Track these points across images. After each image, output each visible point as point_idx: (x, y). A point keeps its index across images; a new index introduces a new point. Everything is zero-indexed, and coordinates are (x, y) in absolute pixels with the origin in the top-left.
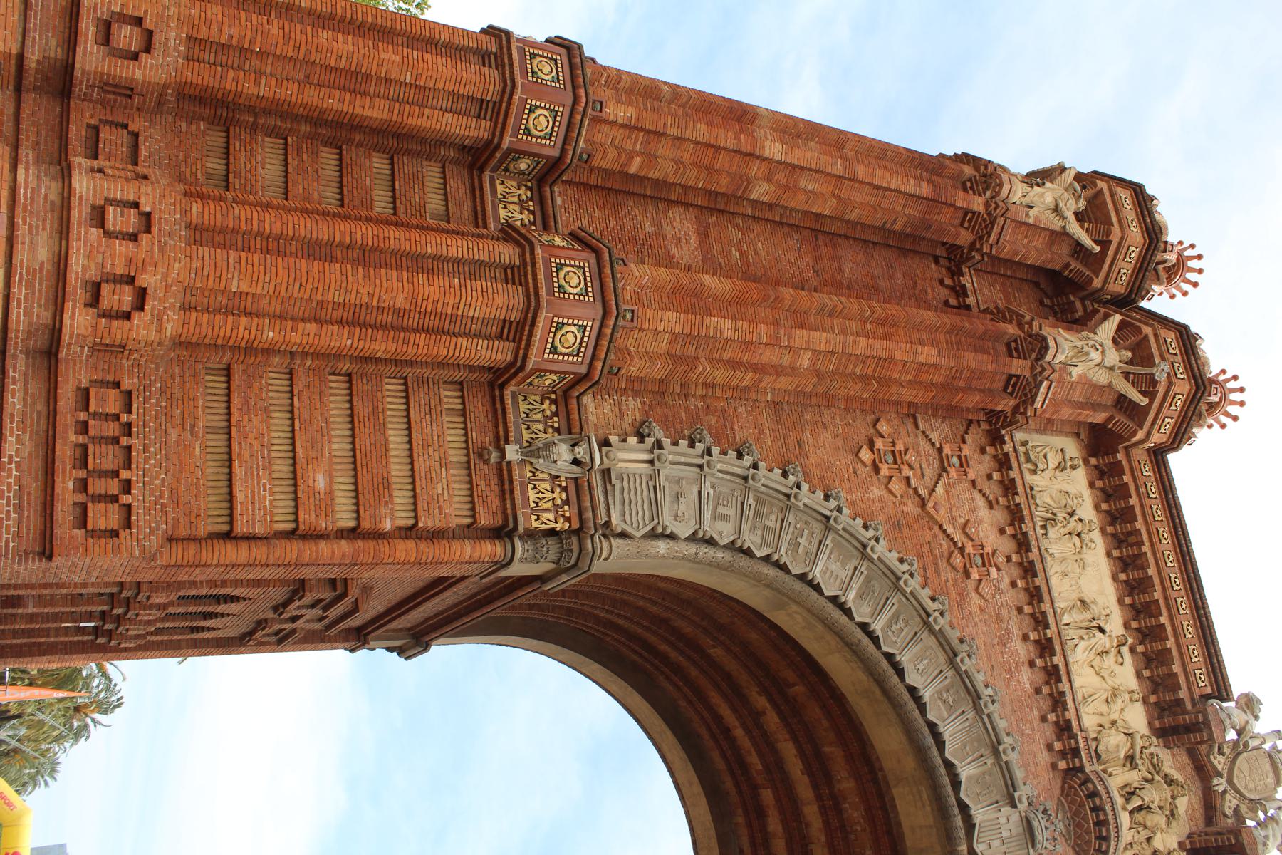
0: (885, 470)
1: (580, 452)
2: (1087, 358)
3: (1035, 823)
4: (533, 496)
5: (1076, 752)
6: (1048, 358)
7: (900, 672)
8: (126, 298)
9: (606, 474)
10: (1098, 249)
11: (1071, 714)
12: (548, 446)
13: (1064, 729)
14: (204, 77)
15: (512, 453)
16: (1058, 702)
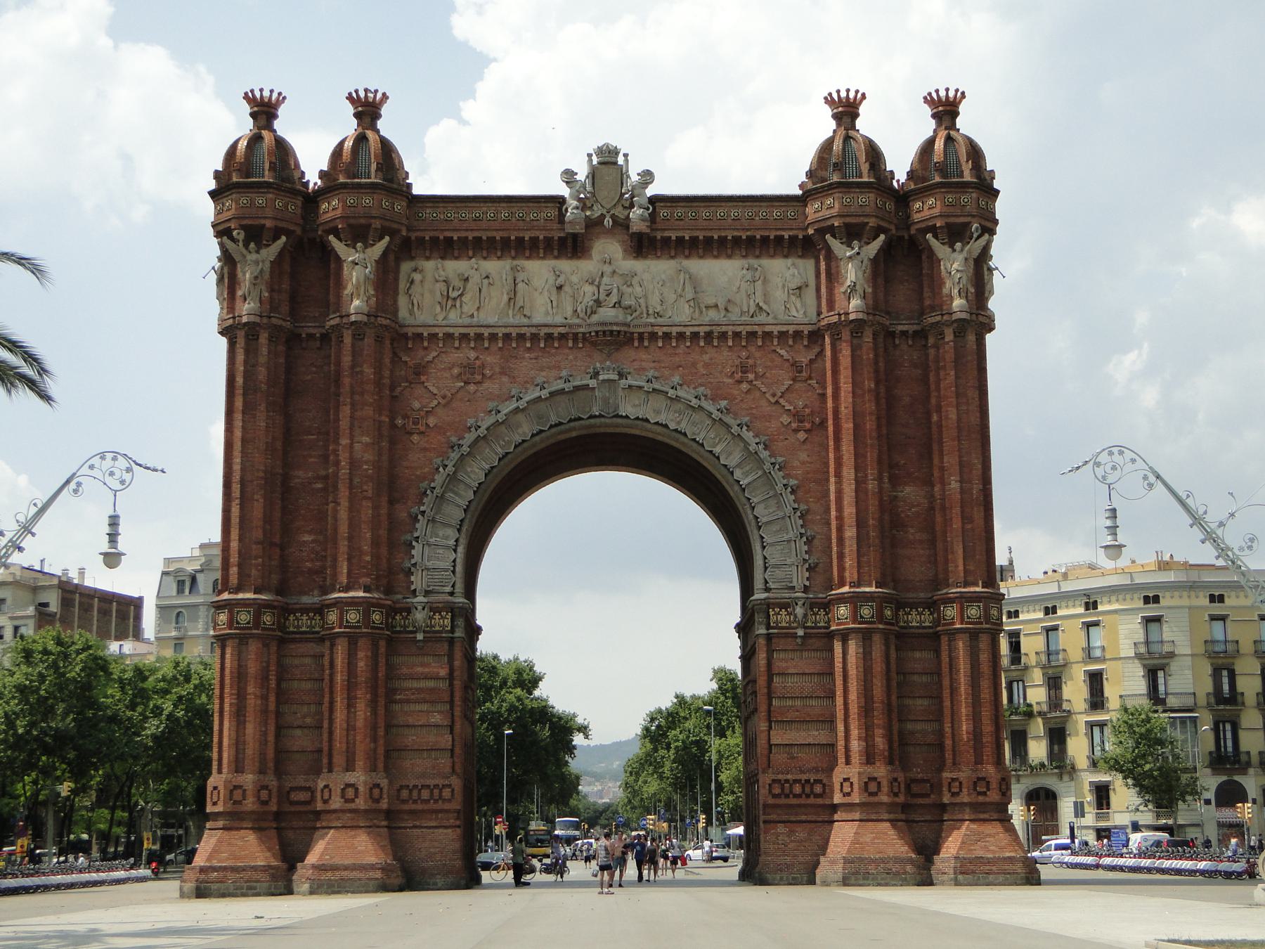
0: (422, 429)
1: (420, 608)
2: (357, 266)
3: (606, 377)
4: (437, 628)
5: (575, 335)
6: (365, 319)
7: (524, 441)
8: (376, 791)
9: (427, 593)
10: (284, 238)
11: (556, 331)
12: (415, 621)
13: (563, 337)
14: (271, 765)
15: (420, 636)
16: (549, 337)
